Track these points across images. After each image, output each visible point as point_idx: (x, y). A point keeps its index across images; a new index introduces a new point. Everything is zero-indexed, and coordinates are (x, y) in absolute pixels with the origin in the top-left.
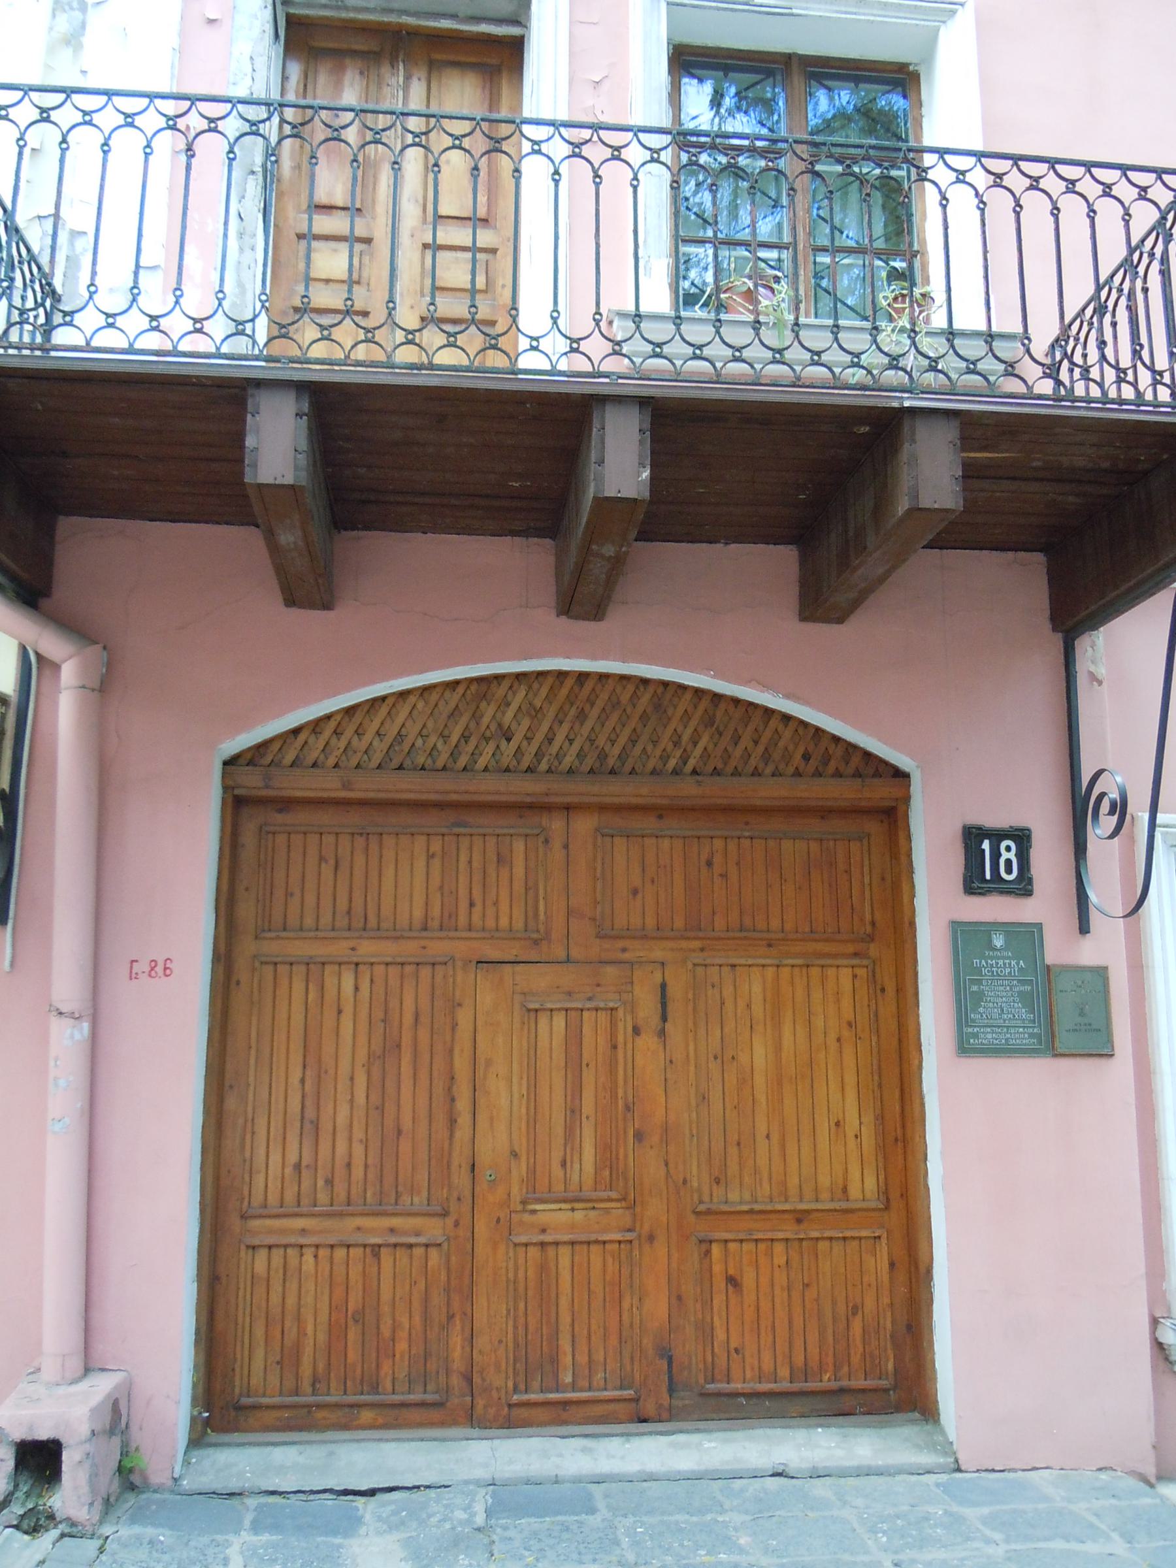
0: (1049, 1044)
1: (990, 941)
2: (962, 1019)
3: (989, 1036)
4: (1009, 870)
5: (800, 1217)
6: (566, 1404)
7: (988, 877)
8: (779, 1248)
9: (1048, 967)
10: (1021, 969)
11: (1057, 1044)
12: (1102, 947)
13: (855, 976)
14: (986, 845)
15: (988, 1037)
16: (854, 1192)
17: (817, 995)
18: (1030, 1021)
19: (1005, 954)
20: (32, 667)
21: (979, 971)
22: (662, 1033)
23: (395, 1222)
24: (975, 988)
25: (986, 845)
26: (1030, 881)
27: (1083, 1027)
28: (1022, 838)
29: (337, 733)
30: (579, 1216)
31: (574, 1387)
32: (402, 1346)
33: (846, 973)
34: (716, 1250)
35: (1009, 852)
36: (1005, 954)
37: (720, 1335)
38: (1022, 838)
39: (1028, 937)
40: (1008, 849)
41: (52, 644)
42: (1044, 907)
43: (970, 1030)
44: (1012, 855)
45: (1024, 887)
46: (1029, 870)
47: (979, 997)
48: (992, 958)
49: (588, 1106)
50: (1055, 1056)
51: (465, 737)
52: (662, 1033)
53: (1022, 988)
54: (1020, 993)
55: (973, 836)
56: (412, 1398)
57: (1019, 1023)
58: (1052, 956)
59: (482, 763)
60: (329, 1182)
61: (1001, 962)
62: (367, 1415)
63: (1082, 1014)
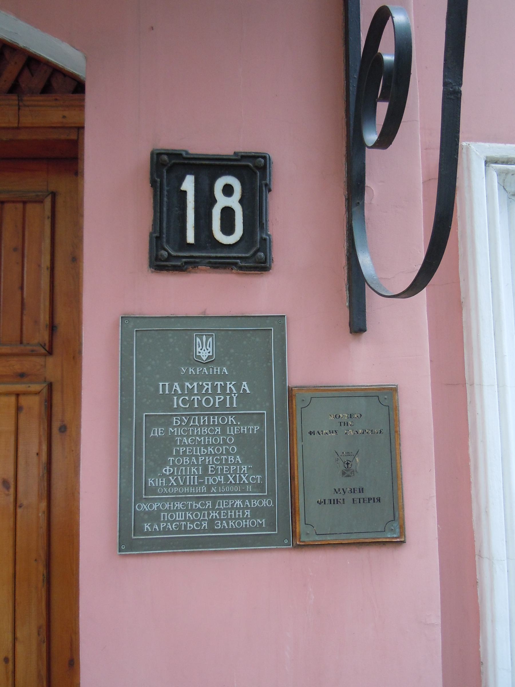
0: (287, 528)
1: (190, 347)
3: (179, 516)
4: (228, 227)
7: (190, 238)
9: (290, 390)
10: (243, 396)
11: (301, 527)
12: (394, 352)
13: (19, 409)
14: (189, 184)
15: (178, 517)
18: (260, 487)
19: (217, 370)
24: (158, 432)
25: (189, 184)
26: (265, 244)
27: (349, 497)
28: (253, 171)
35: (228, 196)
36: (217, 370)
38: (253, 171)
39: (258, 341)
40: (228, 190)
42: (289, 289)
43: (145, 507)
44: (234, 202)
45: (254, 256)
46: (263, 226)
47: (163, 450)
48: (192, 378)
53: (244, 429)
54: (239, 436)
55: (167, 167)
58: (298, 375)
61: (208, 386)
63: (348, 471)
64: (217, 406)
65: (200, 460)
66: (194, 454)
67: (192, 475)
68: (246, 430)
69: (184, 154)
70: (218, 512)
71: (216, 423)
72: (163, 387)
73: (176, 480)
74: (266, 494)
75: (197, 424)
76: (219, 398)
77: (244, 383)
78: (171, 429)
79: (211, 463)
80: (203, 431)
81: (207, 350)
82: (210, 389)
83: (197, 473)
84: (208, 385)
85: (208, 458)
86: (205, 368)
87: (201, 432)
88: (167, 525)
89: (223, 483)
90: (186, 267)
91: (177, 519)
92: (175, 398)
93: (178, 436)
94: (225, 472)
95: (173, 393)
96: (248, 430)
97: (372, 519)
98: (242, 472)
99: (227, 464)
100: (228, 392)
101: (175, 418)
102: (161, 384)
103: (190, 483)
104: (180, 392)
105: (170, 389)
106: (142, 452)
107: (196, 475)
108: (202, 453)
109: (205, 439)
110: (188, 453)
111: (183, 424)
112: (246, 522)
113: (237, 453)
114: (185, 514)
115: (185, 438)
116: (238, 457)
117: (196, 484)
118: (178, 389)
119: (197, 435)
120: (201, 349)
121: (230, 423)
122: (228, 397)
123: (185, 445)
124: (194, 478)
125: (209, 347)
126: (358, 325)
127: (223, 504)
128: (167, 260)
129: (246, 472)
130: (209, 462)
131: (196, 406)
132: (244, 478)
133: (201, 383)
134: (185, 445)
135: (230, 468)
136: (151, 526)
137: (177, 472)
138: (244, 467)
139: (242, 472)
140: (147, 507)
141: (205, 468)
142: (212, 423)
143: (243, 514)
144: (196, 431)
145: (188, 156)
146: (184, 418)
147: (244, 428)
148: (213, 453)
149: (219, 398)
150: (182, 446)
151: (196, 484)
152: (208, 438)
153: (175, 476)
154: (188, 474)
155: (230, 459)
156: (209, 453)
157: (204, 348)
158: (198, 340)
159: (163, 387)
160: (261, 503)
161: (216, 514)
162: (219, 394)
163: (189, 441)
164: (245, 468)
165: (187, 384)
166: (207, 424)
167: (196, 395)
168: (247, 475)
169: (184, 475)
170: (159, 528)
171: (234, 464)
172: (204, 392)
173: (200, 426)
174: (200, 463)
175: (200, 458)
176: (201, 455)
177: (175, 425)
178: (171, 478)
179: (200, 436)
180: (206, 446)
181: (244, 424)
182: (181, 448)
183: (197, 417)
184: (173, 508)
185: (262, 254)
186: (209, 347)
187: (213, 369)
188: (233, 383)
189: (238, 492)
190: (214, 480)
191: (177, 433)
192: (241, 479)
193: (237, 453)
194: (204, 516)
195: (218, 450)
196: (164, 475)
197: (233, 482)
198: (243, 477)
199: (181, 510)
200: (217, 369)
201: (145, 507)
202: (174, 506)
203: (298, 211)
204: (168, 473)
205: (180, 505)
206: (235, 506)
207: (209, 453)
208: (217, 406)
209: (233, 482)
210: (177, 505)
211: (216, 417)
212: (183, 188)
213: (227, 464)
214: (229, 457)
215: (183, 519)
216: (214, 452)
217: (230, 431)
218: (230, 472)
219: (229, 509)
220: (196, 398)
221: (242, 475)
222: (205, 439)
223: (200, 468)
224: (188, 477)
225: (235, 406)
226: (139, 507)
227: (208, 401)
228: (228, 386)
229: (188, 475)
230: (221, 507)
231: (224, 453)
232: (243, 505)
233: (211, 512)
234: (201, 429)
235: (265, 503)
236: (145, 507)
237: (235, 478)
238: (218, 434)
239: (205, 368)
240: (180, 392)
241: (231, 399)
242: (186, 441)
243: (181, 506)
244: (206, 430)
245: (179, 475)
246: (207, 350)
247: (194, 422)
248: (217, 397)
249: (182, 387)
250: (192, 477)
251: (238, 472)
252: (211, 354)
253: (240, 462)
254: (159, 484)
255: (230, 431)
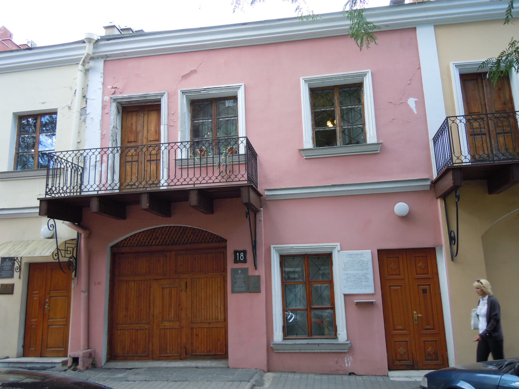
0: (249, 290)
2: (233, 286)
5: (209, 323)
6: (168, 356)
8: (205, 329)
15: (237, 289)
16: (219, 318)
17: (214, 283)
20: (79, 235)
22: (186, 291)
23: (141, 325)
29: (129, 240)
30: (171, 324)
31: (170, 353)
32: (141, 346)
33: (219, 278)
34: (194, 330)
35: (242, 255)
37: (195, 345)
38: (245, 252)
39: (245, 271)
41: (81, 231)
45: (245, 261)
47: (235, 282)
49: (173, 305)
50: (250, 292)
51: (151, 239)
52: (186, 291)
55: (235, 252)
56: (143, 355)
59: (154, 243)
60: (130, 319)
62: (136, 358)
97: (257, 290)
106: (234, 283)
126: (256, 269)
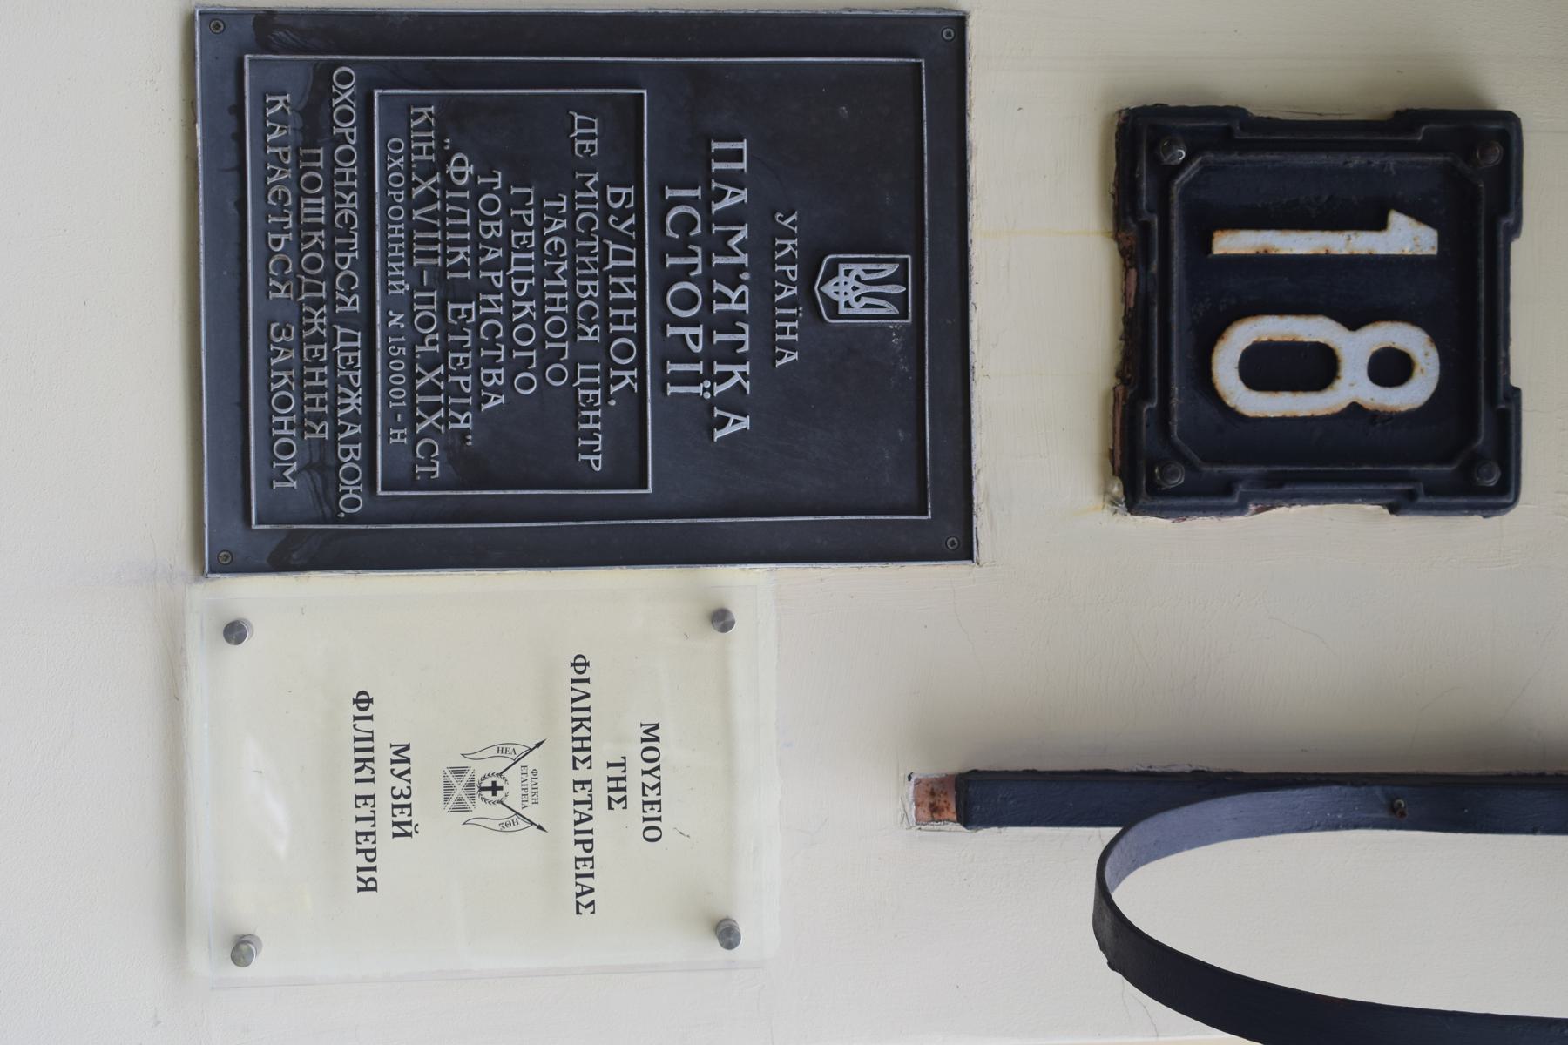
1: (868, 244)
4: (1264, 367)
7: (1230, 243)
10: (706, 416)
14: (1406, 237)
19: (789, 330)
21: (690, 163)
24: (586, 136)
25: (1406, 237)
35: (1371, 368)
44: (1354, 387)
45: (1168, 452)
54: (573, 404)
57: (393, 390)
61: (737, 300)
64: (671, 331)
65: (493, 275)
66: (514, 256)
67: (444, 249)
68: (591, 425)
69: (1511, 220)
70: (324, 332)
71: (613, 328)
72: (735, 154)
73: (429, 198)
74: (380, 492)
75: (612, 263)
76: (695, 338)
77: (746, 423)
78: (596, 178)
79: (483, 310)
80: (588, 283)
81: (858, 299)
82: (724, 307)
83: (449, 263)
84: (741, 299)
85: (498, 302)
86: (795, 291)
87: (583, 278)
88: (286, 167)
89: (419, 349)
90: (1134, 226)
91: (304, 201)
92: (698, 193)
93: (571, 204)
94: (451, 355)
95: (714, 185)
96: (590, 435)
98: (451, 413)
99: (480, 363)
100: (718, 368)
101: (632, 190)
102: (743, 145)
103: (421, 241)
104: (716, 207)
105: (724, 177)
107: (444, 262)
108: (514, 282)
109: (561, 290)
110: (514, 234)
111: (612, 218)
112: (291, 426)
113: (514, 400)
114: (318, 227)
115: (564, 224)
116: (502, 400)
117: (417, 262)
118: (727, 202)
119: (573, 266)
120: (858, 278)
121: (613, 373)
122: (699, 367)
123: (541, 225)
124: (434, 254)
125: (867, 306)
127: (349, 347)
128: (1155, 161)
129: (451, 426)
130: (488, 304)
131: (670, 261)
132: (430, 421)
133: (745, 276)
134: (541, 225)
135: (466, 374)
136: (281, 118)
137: (453, 201)
138: (467, 421)
139: (451, 413)
140: (345, 102)
141: (466, 292)
142: (612, 312)
143: (318, 418)
144: (587, 260)
145: (1501, 235)
146: (632, 220)
147: (596, 420)
148: (516, 317)
149: (695, 338)
150: (539, 216)
151: (417, 262)
152: (563, 302)
153: (444, 194)
154: (449, 236)
155: (494, 372)
156: (515, 304)
157: (864, 289)
158: (890, 269)
159: (735, 154)
160: (351, 474)
161: (316, 328)
162: (708, 336)
163: (556, 240)
164: (465, 421)
165: (743, 233)
166: (612, 296)
167: (707, 260)
168: (442, 428)
169: (444, 222)
170: (274, 144)
171: (478, 386)
172: (717, 287)
173: (604, 277)
174: (482, 274)
175: (500, 274)
176: (508, 280)
177: (610, 190)
178: (437, 178)
179: (571, 275)
180: (537, 293)
181: (608, 419)
182: (532, 212)
183: (633, 263)
184: (339, 188)
185: (1179, 480)
186: (867, 306)
187: (792, 318)
188: (747, 385)
189: (387, 400)
190: (427, 322)
191: (582, 200)
192: (431, 409)
193: (514, 400)
194: (310, 288)
195: (526, 335)
196: (445, 159)
197: (420, 383)
198: (436, 417)
199: (332, 213)
200: (793, 331)
201: (346, 96)
202: (348, 190)
203: (1313, 602)
204: (452, 169)
205: (349, 207)
206: (340, 389)
207: (515, 304)
208: (671, 331)
209: (420, 383)
210: (348, 199)
211: (634, 328)
212: (1397, 220)
213: (480, 363)
214: (501, 371)
215: (304, 220)
216: (519, 322)
217: (585, 374)
218: (454, 374)
219: (335, 369)
220: (698, 260)
221: (441, 413)
222: (561, 290)
223: (468, 275)
224: (438, 235)
225: (671, 389)
226: (345, 79)
227: (687, 300)
228: (736, 369)
229: (444, 235)
230: (340, 345)
231: (516, 354)
232: (343, 418)
233: (324, 309)
234: (593, 278)
235: (351, 488)
236: (346, 96)
237: (432, 389)
238: (575, 332)
239: (795, 291)
240: (716, 207)
241: (695, 379)
242: (554, 228)
243: (346, 212)
244: (592, 289)
245: (444, 207)
246: (858, 299)
247: (619, 255)
248: (699, 331)
249: (734, 217)
250: (438, 248)
251: (451, 401)
252: (843, 310)
253: (484, 407)
254: (418, 140)
255: (585, 374)
